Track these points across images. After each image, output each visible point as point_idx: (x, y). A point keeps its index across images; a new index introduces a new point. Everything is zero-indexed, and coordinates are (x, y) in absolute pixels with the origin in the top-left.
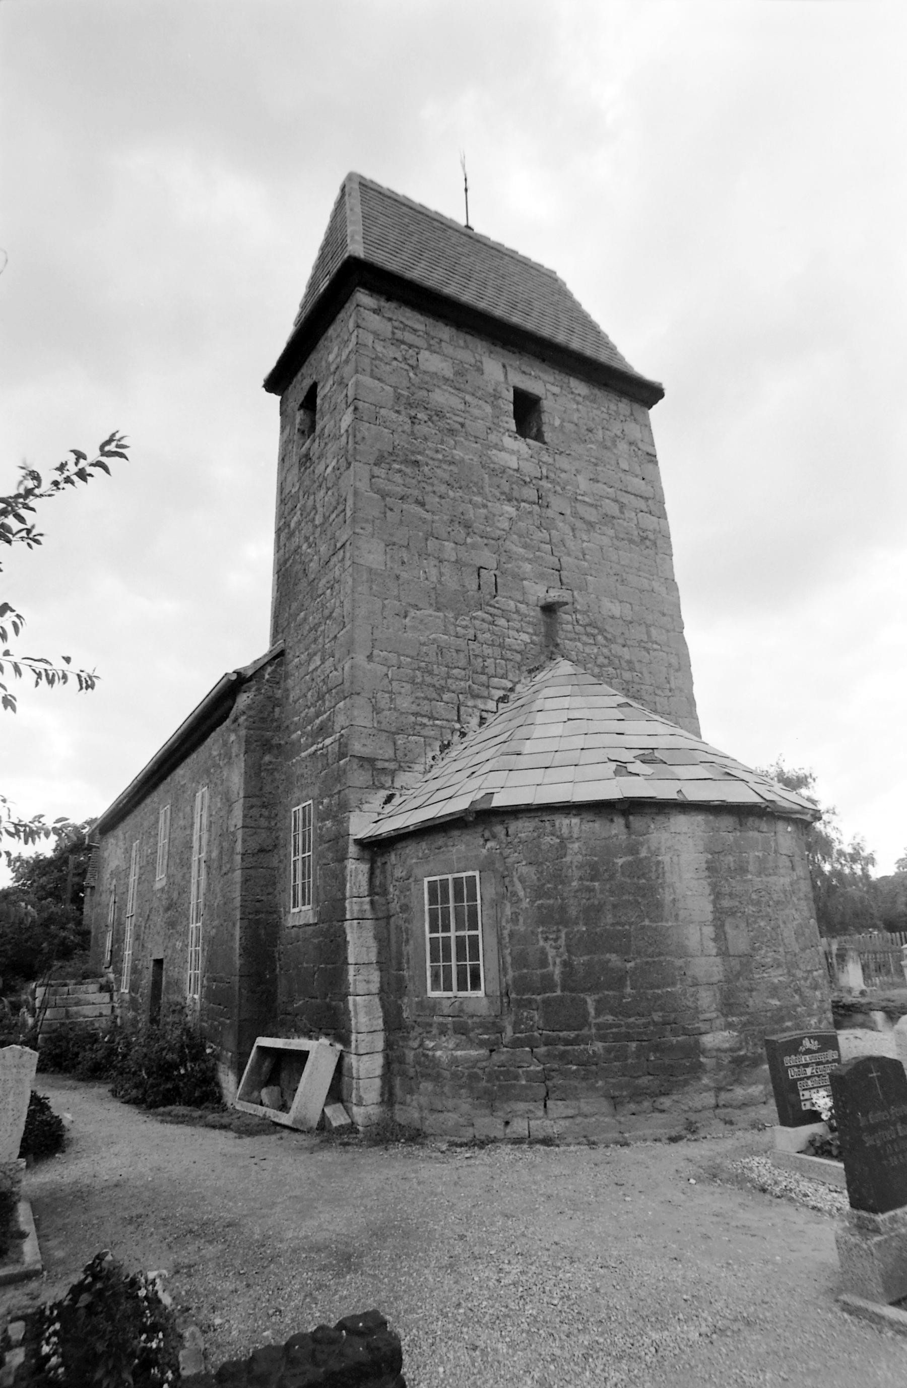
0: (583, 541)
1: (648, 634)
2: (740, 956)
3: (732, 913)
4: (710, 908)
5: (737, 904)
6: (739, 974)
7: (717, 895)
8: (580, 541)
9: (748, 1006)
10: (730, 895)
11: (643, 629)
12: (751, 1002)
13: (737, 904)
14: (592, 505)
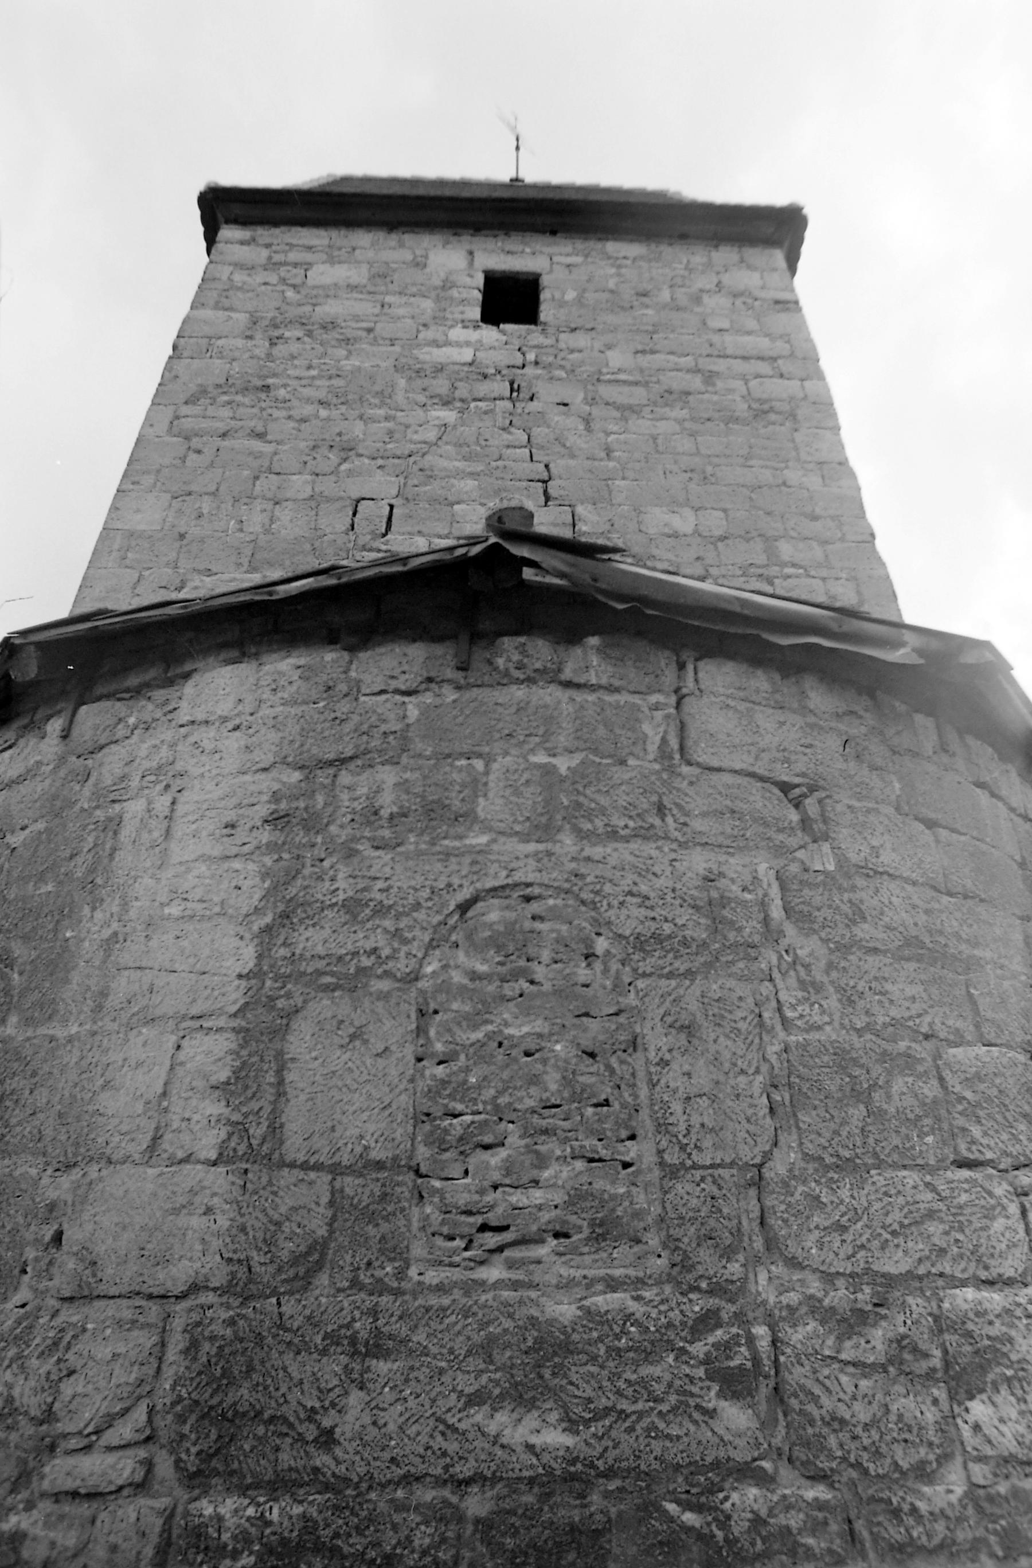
0: (608, 434)
1: (771, 553)
2: (336, 1170)
3: (348, 979)
4: (249, 953)
5: (379, 939)
6: (312, 1259)
7: (285, 912)
8: (601, 435)
9: (327, 1439)
10: (352, 907)
11: (758, 545)
12: (353, 1416)
13: (379, 939)
14: (636, 383)
